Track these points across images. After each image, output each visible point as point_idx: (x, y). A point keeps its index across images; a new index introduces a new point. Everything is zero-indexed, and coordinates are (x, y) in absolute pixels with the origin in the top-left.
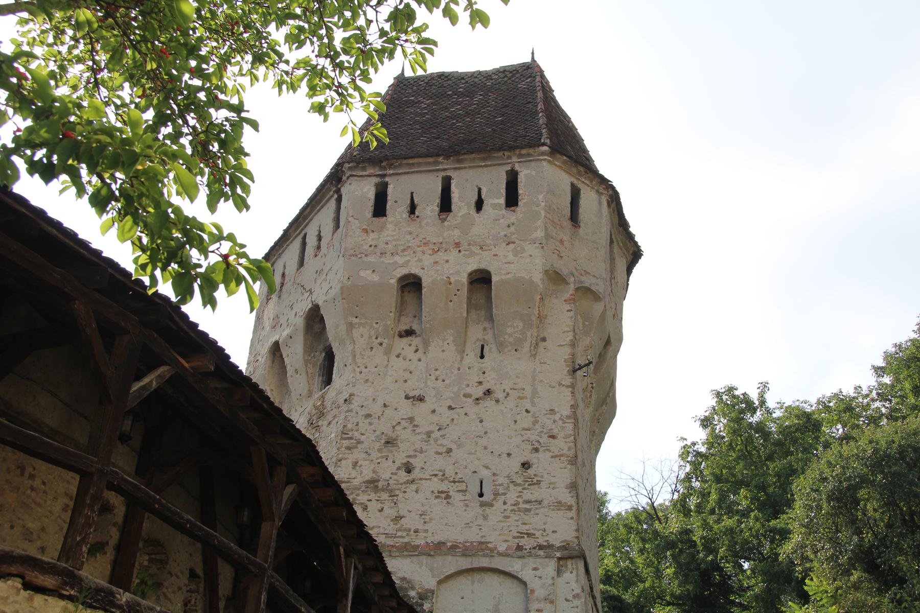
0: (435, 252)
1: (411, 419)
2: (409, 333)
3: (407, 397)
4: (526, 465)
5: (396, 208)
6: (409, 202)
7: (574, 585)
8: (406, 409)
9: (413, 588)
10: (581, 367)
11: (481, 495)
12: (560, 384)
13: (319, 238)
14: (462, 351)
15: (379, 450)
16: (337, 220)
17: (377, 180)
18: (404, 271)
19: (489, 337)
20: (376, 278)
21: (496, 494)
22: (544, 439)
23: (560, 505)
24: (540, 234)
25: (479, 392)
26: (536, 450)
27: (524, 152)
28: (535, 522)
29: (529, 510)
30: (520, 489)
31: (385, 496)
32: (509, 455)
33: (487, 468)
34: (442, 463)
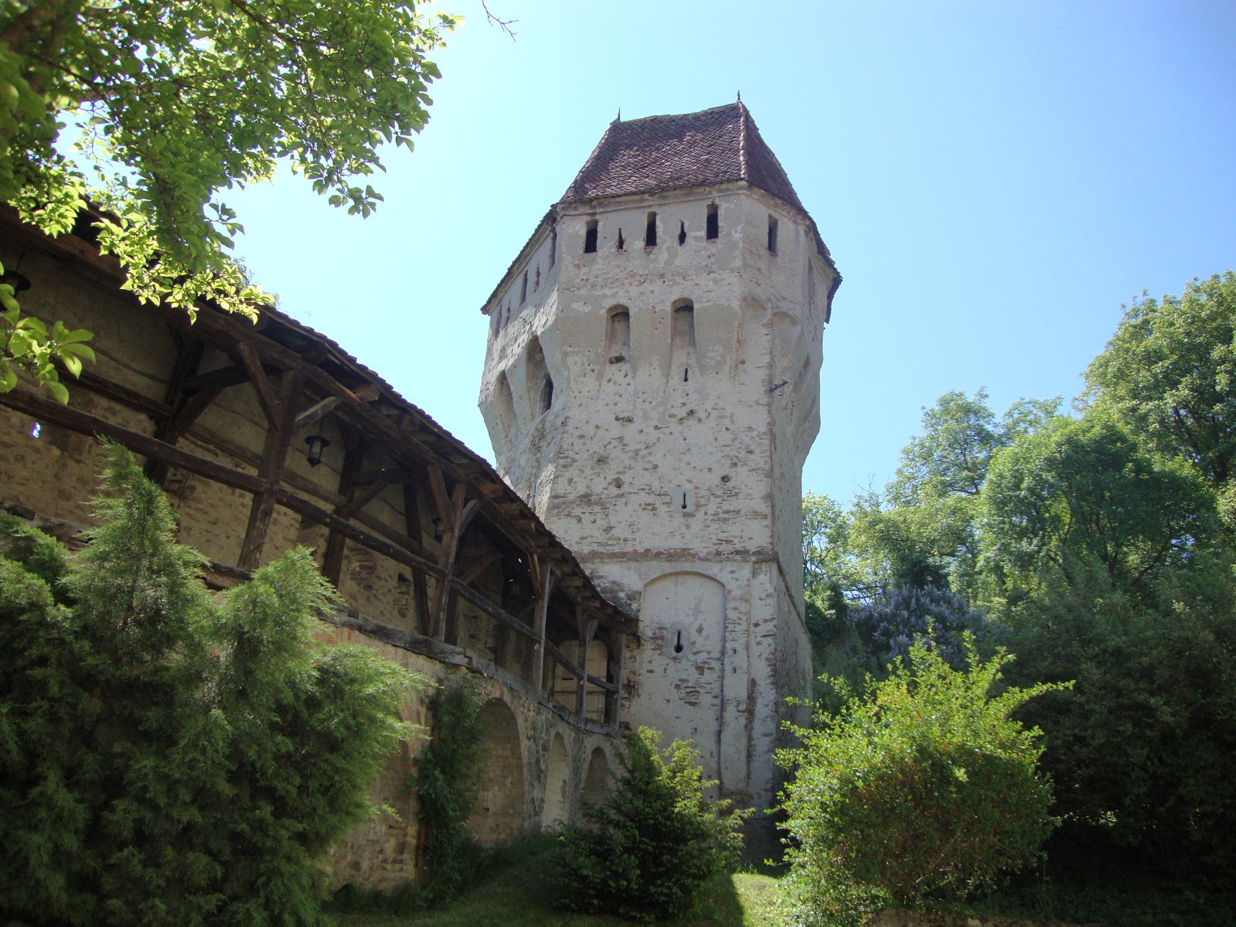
0: (641, 283)
1: (621, 439)
2: (619, 359)
3: (617, 419)
4: (725, 479)
5: (606, 245)
6: (617, 237)
7: (768, 585)
8: (616, 430)
9: (622, 590)
10: (777, 387)
11: (684, 507)
12: (758, 403)
13: (538, 274)
14: (667, 376)
15: (592, 468)
16: (553, 257)
17: (588, 218)
18: (613, 302)
19: (693, 361)
20: (587, 309)
21: (698, 506)
23: (756, 514)
24: (738, 263)
25: (683, 412)
26: (735, 465)
27: (723, 187)
28: (733, 530)
29: (728, 519)
30: (719, 500)
31: (597, 509)
32: (710, 470)
33: (689, 481)
34: (646, 478)
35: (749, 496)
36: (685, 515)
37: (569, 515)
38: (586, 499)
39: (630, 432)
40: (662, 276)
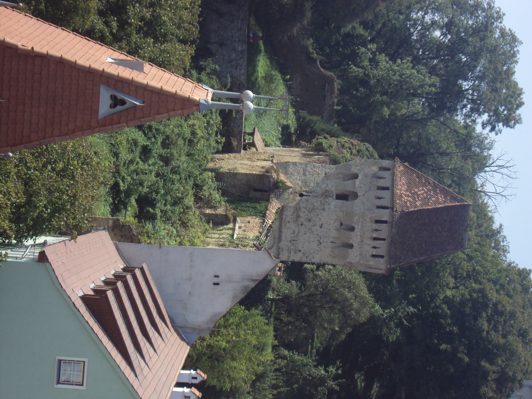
1: (315, 225)
2: (341, 224)
8: (318, 224)
14: (333, 238)
19: (337, 245)
20: (355, 221)
22: (306, 255)
23: (289, 257)
24: (361, 262)
25: (321, 241)
35: (294, 256)
36: (291, 241)
37: (294, 212)
38: (298, 216)
39: (317, 227)
40: (362, 241)
